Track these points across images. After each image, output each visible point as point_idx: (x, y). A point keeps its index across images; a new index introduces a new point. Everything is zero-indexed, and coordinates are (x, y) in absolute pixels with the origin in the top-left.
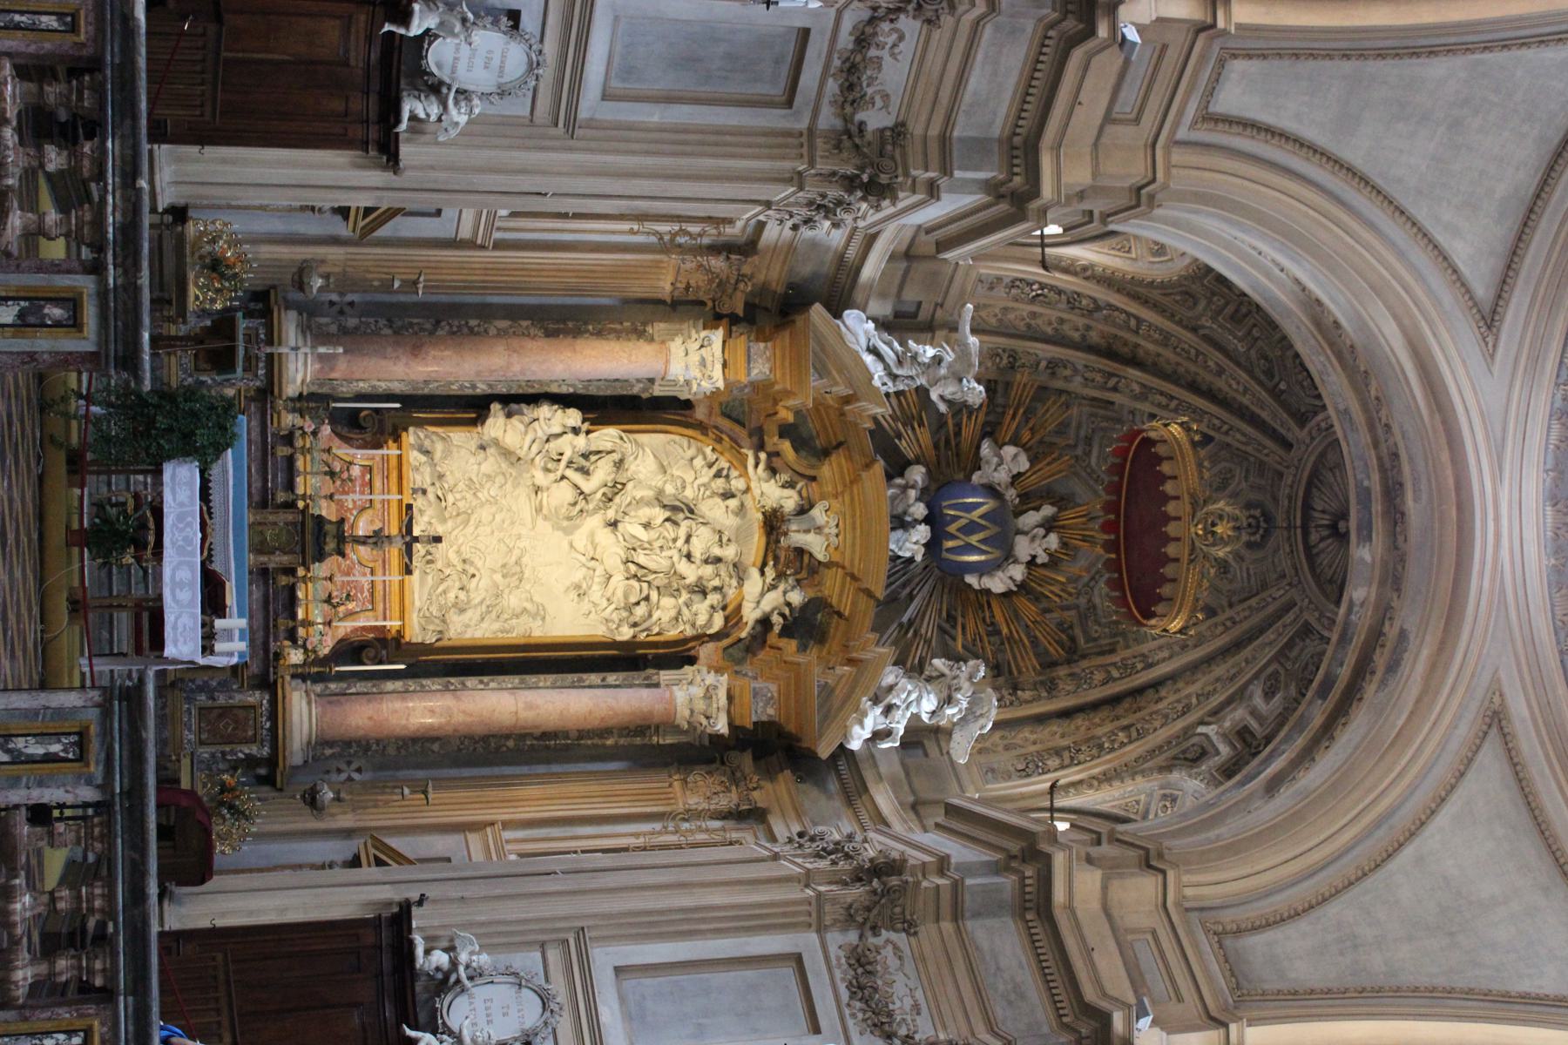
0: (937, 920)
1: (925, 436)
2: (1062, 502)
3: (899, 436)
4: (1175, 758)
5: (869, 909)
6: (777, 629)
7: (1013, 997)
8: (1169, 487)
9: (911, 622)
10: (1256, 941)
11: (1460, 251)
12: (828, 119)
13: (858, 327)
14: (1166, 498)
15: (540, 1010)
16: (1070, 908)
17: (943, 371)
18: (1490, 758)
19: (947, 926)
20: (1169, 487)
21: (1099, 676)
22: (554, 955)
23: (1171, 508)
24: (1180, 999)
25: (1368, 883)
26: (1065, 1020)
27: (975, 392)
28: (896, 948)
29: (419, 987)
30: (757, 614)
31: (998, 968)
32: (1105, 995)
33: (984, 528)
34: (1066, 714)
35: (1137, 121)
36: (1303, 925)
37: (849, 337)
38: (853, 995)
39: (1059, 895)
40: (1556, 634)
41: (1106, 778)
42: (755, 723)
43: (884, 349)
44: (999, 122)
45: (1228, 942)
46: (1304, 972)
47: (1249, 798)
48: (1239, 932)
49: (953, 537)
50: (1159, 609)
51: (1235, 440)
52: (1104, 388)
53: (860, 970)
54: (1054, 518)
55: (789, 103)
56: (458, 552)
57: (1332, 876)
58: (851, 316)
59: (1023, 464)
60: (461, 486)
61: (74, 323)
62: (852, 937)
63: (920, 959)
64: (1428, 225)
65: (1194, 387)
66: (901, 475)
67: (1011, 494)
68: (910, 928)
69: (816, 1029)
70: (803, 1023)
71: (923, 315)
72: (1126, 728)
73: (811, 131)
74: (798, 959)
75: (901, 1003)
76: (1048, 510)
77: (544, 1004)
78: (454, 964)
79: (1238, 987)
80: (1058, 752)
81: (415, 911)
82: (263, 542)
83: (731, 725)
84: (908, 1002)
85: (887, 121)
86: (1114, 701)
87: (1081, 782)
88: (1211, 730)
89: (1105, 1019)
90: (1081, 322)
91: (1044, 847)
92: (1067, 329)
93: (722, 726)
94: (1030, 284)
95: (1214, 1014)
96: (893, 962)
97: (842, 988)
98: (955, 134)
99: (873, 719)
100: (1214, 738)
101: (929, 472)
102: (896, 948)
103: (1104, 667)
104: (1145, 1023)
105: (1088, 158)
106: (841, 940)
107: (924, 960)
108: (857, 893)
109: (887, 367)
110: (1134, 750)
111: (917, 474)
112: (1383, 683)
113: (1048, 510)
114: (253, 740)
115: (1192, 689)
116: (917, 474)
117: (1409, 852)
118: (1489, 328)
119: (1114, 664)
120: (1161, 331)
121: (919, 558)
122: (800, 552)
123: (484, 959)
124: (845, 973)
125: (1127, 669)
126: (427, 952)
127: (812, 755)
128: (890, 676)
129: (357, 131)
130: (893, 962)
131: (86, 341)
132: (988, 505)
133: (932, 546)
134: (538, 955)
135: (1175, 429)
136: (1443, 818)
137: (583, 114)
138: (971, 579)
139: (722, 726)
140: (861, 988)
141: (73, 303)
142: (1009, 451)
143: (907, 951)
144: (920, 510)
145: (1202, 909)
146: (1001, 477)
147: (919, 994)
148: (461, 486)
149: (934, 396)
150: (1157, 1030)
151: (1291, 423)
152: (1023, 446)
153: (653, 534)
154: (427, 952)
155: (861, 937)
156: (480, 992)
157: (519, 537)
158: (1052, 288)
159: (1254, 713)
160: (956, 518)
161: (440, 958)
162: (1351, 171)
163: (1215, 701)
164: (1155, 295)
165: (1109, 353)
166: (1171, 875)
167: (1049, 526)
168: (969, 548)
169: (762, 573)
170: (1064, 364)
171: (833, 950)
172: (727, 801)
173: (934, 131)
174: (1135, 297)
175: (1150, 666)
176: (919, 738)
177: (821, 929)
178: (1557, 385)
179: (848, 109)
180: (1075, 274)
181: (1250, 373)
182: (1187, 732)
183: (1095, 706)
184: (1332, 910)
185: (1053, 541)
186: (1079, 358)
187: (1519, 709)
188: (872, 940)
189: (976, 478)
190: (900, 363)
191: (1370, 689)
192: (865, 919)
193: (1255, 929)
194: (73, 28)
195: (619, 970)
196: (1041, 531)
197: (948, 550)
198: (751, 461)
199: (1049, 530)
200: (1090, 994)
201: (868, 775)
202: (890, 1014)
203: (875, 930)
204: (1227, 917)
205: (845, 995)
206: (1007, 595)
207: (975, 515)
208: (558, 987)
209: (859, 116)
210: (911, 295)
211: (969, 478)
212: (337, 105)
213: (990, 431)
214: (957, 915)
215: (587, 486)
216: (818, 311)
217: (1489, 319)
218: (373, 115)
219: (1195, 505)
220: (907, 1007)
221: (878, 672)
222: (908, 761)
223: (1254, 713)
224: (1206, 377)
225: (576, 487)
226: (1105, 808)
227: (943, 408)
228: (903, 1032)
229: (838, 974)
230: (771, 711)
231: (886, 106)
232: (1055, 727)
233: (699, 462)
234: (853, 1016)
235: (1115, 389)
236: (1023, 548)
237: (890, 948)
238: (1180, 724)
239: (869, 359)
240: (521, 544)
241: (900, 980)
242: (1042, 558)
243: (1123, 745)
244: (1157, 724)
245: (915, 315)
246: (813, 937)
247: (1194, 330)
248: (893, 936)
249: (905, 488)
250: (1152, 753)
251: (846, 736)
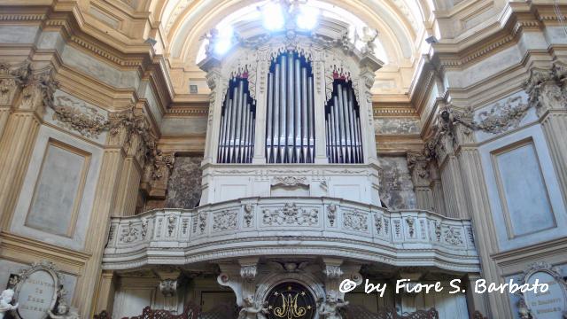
7: (101, 73)
15: (45, 274)
16: (85, 23)
24: (122, 20)
26: (123, 64)
28: (63, 98)
31: (88, 68)
38: (79, 130)
53: (69, 119)
63: (72, 93)
69: (88, 154)
75: (91, 117)
84: (89, 111)
95: (135, 16)
97: (73, 131)
107: (74, 92)
124: (67, 126)
130: (69, 104)
140: (77, 125)
147: (88, 105)
155: (53, 108)
177: (42, 122)
195: (25, 225)
205: (77, 133)
208: (36, 261)
220: (92, 113)
234: (88, 136)
237: (62, 100)
241: (77, 107)
246: (43, 126)
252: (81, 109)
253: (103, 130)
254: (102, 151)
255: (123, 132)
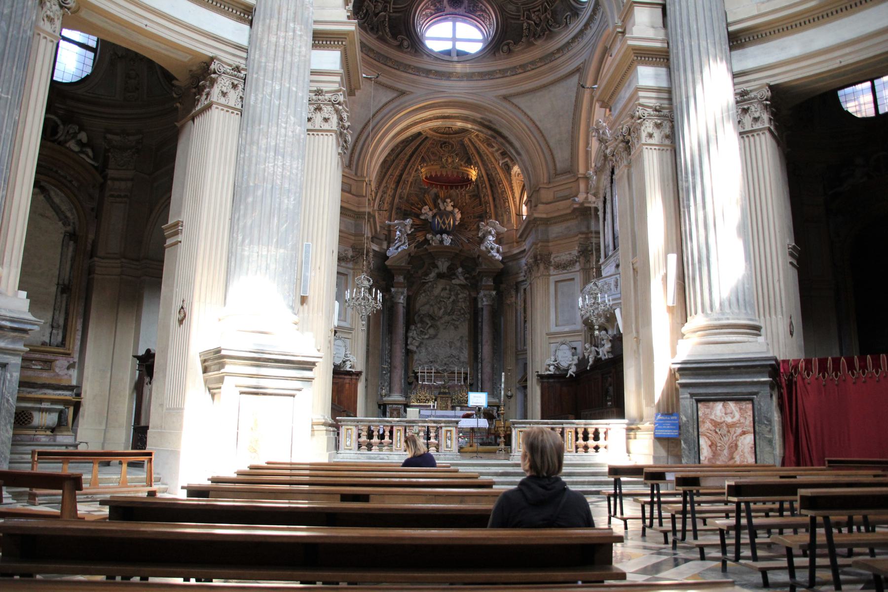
0: (548, 246)
1: (419, 234)
2: (437, 197)
3: (419, 241)
4: (508, 172)
5: (545, 264)
6: (468, 276)
8: (439, 174)
9: (468, 240)
10: (558, 165)
11: (385, 100)
12: (350, 265)
13: (392, 252)
14: (442, 175)
17: (403, 230)
18: (515, 101)
19: (550, 244)
20: (439, 174)
21: (484, 190)
22: (552, 341)
23: (444, 174)
25: (545, 134)
26: (575, 217)
27: (409, 221)
28: (555, 257)
29: (557, 373)
30: (464, 281)
32: (570, 207)
33: (444, 219)
34: (494, 199)
35: (351, 185)
36: (555, 152)
37: (394, 255)
38: (566, 269)
39: (544, 216)
40: (484, 80)
41: (512, 190)
42: (494, 283)
43: (397, 245)
44: (349, 220)
45: (558, 172)
46: (566, 154)
47: (521, 159)
48: (555, 169)
49: (446, 228)
50: (470, 177)
51: (424, 150)
52: (407, 185)
54: (442, 199)
55: (346, 275)
56: (445, 358)
57: (543, 144)
58: (388, 254)
59: (426, 207)
60: (428, 357)
61: (450, 431)
62: (552, 268)
64: (377, 108)
65: (409, 161)
66: (429, 241)
67: (435, 211)
68: (550, 254)
69: (573, 279)
70: (571, 282)
71: (386, 233)
72: (499, 184)
73: (353, 269)
74: (556, 282)
76: (439, 201)
77: (564, 344)
78: (553, 365)
79: (569, 172)
80: (505, 203)
81: (539, 373)
82: (445, 407)
83: (494, 290)
84: (568, 256)
85: (351, 249)
86: (491, 186)
87: (513, 197)
88: (501, 162)
89: (575, 209)
90: (390, 190)
91: (532, 218)
92: (391, 194)
93: (494, 293)
94: (380, 204)
96: (558, 259)
98: (353, 232)
99: (494, 253)
100: (503, 161)
101: (429, 233)
102: (555, 257)
103: (482, 188)
104: (577, 199)
105: (360, 198)
106: (552, 271)
108: (542, 266)
109: (402, 245)
110: (505, 183)
111: (429, 236)
112: (494, 124)
113: (439, 201)
114: (493, 411)
115: (490, 166)
116: (429, 236)
117: (538, 123)
118: (404, 93)
119: (482, 185)
120: (394, 169)
121: (451, 237)
122: (449, 268)
123: (553, 358)
125: (484, 182)
126: (550, 371)
127: (502, 269)
128: (483, 248)
129: (354, 381)
130: (558, 259)
131: (453, 429)
132: (437, 219)
133: (448, 234)
134: (552, 345)
135: (423, 170)
136: (529, 113)
137: (349, 326)
138: (457, 223)
139: (494, 293)
140: (564, 267)
141: (447, 431)
142: (423, 211)
143: (556, 255)
144: (438, 236)
145: (549, 179)
146: (430, 214)
147: (567, 253)
148: (428, 357)
149: (409, 232)
150: (579, 196)
151: (420, 137)
152: (422, 207)
153: (443, 307)
154: (550, 371)
155: (552, 266)
156: (560, 359)
157: (442, 342)
158: (381, 199)
159: (497, 151)
160: (441, 226)
161: (552, 368)
162: (364, 128)
163: (493, 160)
164: (384, 171)
165: (398, 183)
166: (541, 186)
167: (444, 201)
168: (449, 224)
169: (454, 279)
170: (400, 194)
171: (555, 273)
172: (513, 293)
173: (353, 238)
174: (384, 176)
175: (482, 176)
176: (499, 241)
177: (550, 275)
178: (420, 76)
179: (348, 260)
180: (377, 192)
181: (406, 146)
182: (502, 168)
183: (492, 191)
184: (551, 144)
185: (448, 200)
186: (399, 191)
187: (503, 92)
188: (553, 263)
189: (430, 220)
190: (401, 241)
191: (494, 127)
192: (548, 264)
193: (555, 165)
194: (400, 430)
195: (556, 326)
196: (445, 203)
197: (449, 228)
198: (424, 281)
199: (445, 201)
200: (569, 211)
201: (508, 254)
202: (571, 261)
203: (550, 262)
204: (552, 172)
206: (462, 213)
207: (440, 222)
208: (559, 340)
209: (350, 257)
210: (383, 237)
211: (430, 222)
212: (347, 386)
213: (417, 216)
214: (548, 241)
215: (430, 324)
216: (387, 263)
217: (403, 93)
218: (350, 377)
219: (443, 167)
221: (482, 251)
222: (505, 242)
223: (497, 151)
224: (407, 157)
225: (429, 327)
226: (520, 192)
227: (413, 230)
228: (575, 258)
229: (560, 272)
230: (490, 280)
231: (347, 250)
232: (497, 201)
233: (423, 295)
235: (408, 181)
236: (450, 208)
238: (499, 171)
239: (400, 250)
240: (444, 342)
241: (562, 257)
242: (452, 203)
243: (503, 185)
244: (498, 176)
245: (386, 235)
246: (551, 278)
247: (394, 161)
248: (552, 258)
249: (433, 240)
250: (506, 178)
251: (498, 260)
252: (564, 257)
253: (576, 261)
254: (578, 273)
255: (582, 259)
